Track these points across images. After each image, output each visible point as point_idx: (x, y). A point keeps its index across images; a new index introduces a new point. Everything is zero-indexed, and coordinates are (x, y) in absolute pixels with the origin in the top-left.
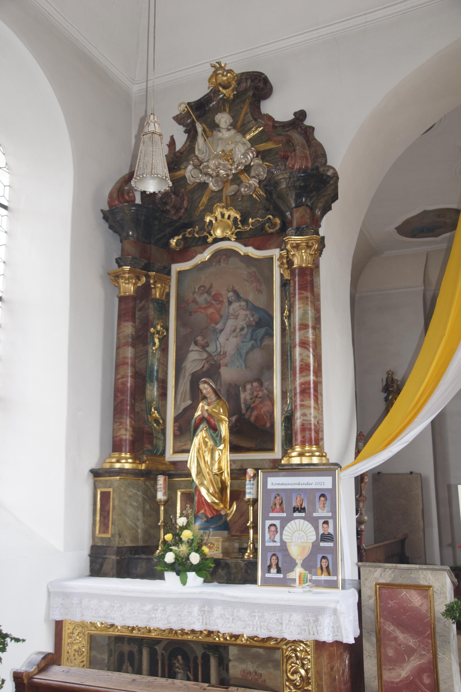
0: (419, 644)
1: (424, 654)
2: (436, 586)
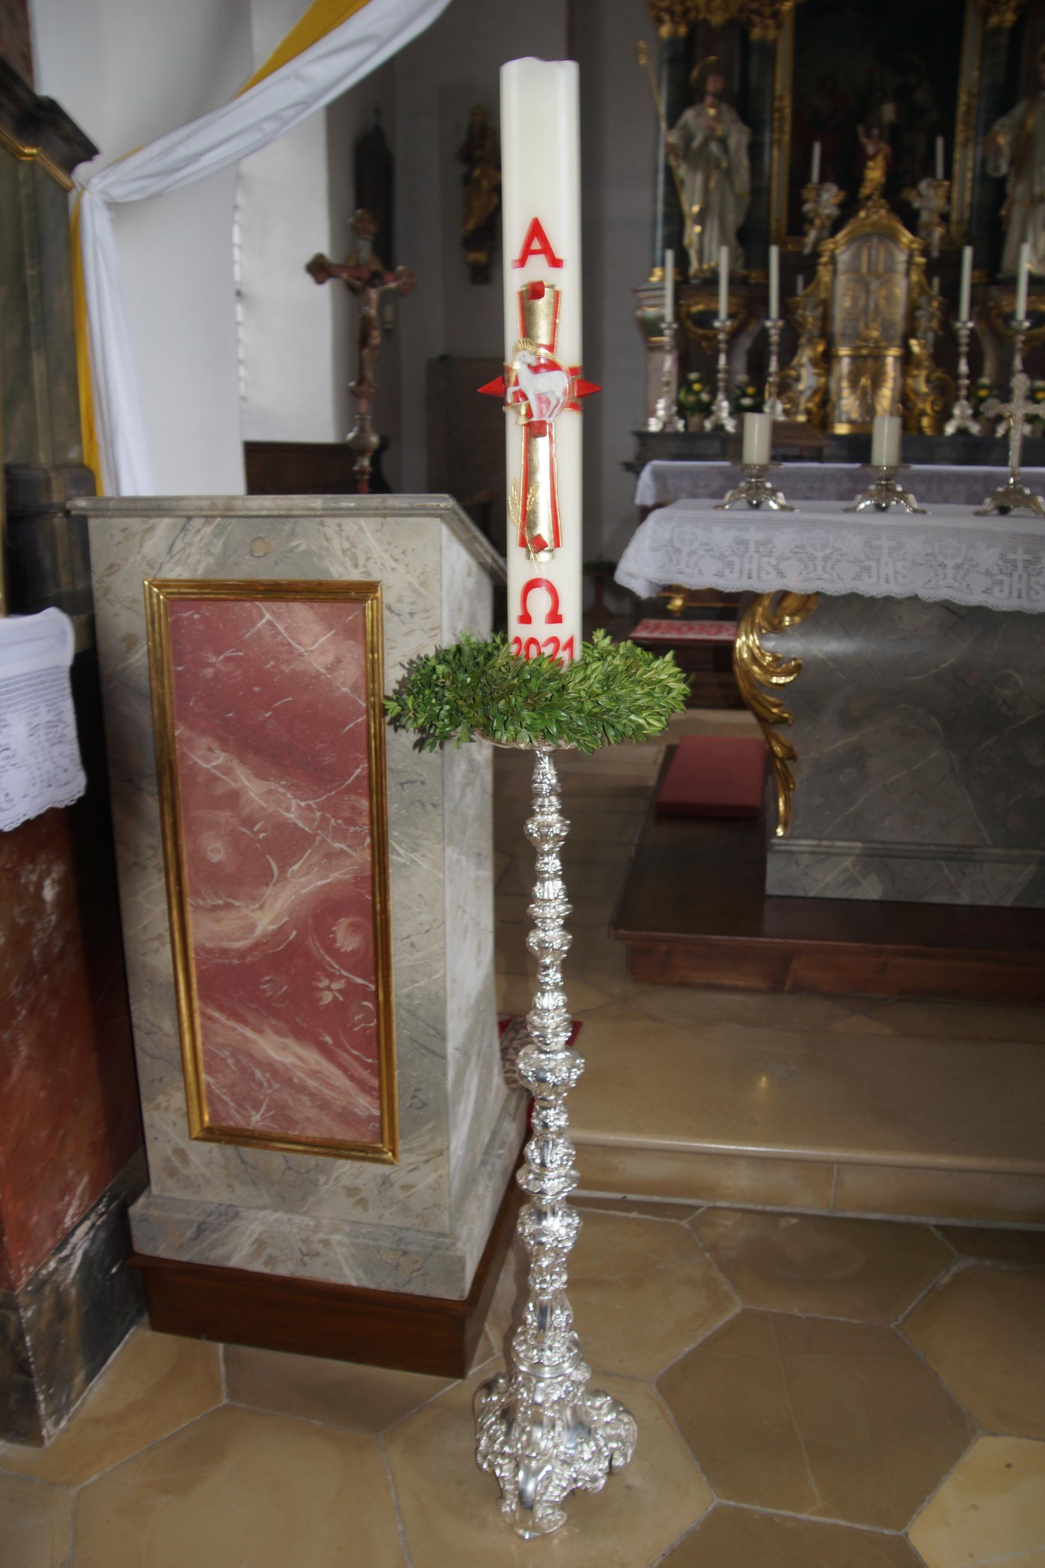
0: (323, 819)
1: (342, 852)
2: (395, 585)
